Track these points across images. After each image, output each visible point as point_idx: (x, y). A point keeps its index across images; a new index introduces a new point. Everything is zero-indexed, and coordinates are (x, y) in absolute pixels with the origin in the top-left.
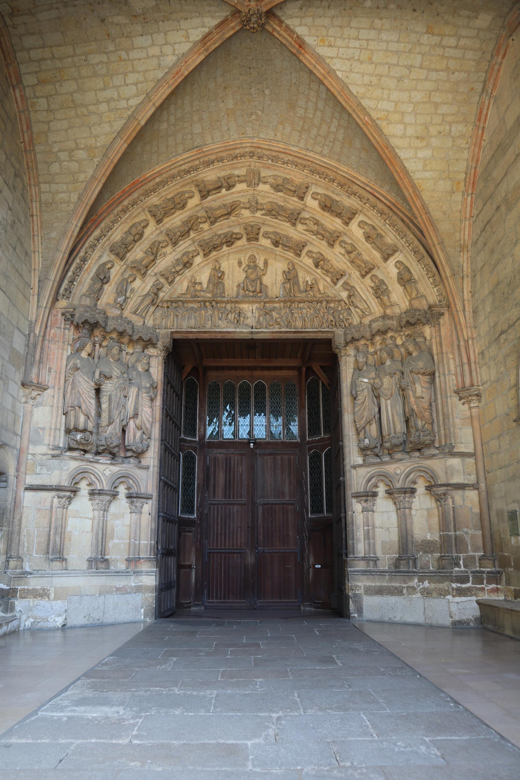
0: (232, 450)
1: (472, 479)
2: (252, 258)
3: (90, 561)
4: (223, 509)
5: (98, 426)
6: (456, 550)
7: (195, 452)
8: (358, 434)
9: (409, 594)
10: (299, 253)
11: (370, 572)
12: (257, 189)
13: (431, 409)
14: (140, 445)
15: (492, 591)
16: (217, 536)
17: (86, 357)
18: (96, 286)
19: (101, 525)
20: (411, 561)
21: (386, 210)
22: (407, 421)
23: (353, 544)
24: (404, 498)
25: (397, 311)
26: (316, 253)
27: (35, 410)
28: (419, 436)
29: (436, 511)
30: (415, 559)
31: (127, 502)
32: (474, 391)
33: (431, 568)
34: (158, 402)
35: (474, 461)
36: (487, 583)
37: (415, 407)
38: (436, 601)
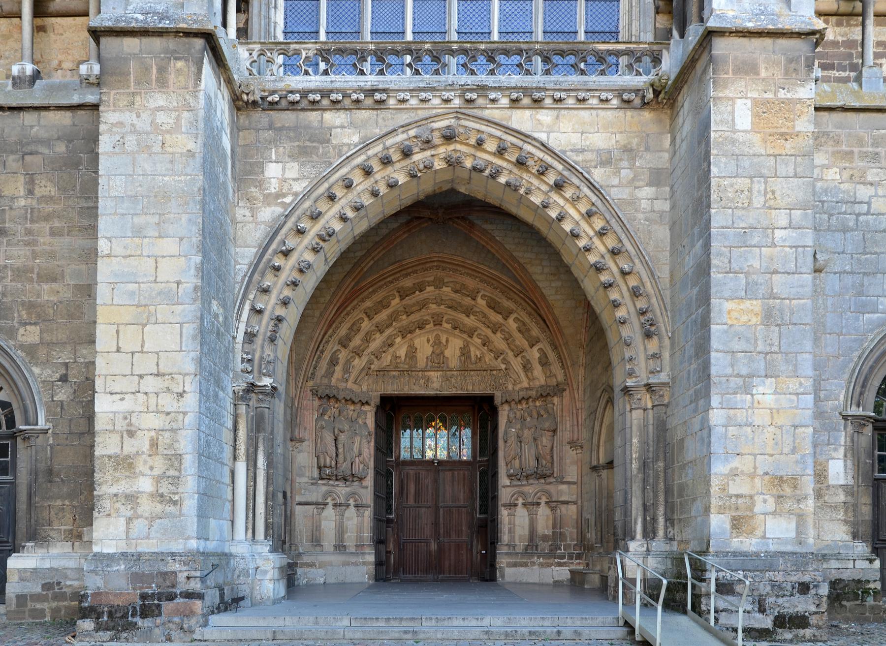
3: (335, 546)
21: (533, 312)
25: (537, 383)
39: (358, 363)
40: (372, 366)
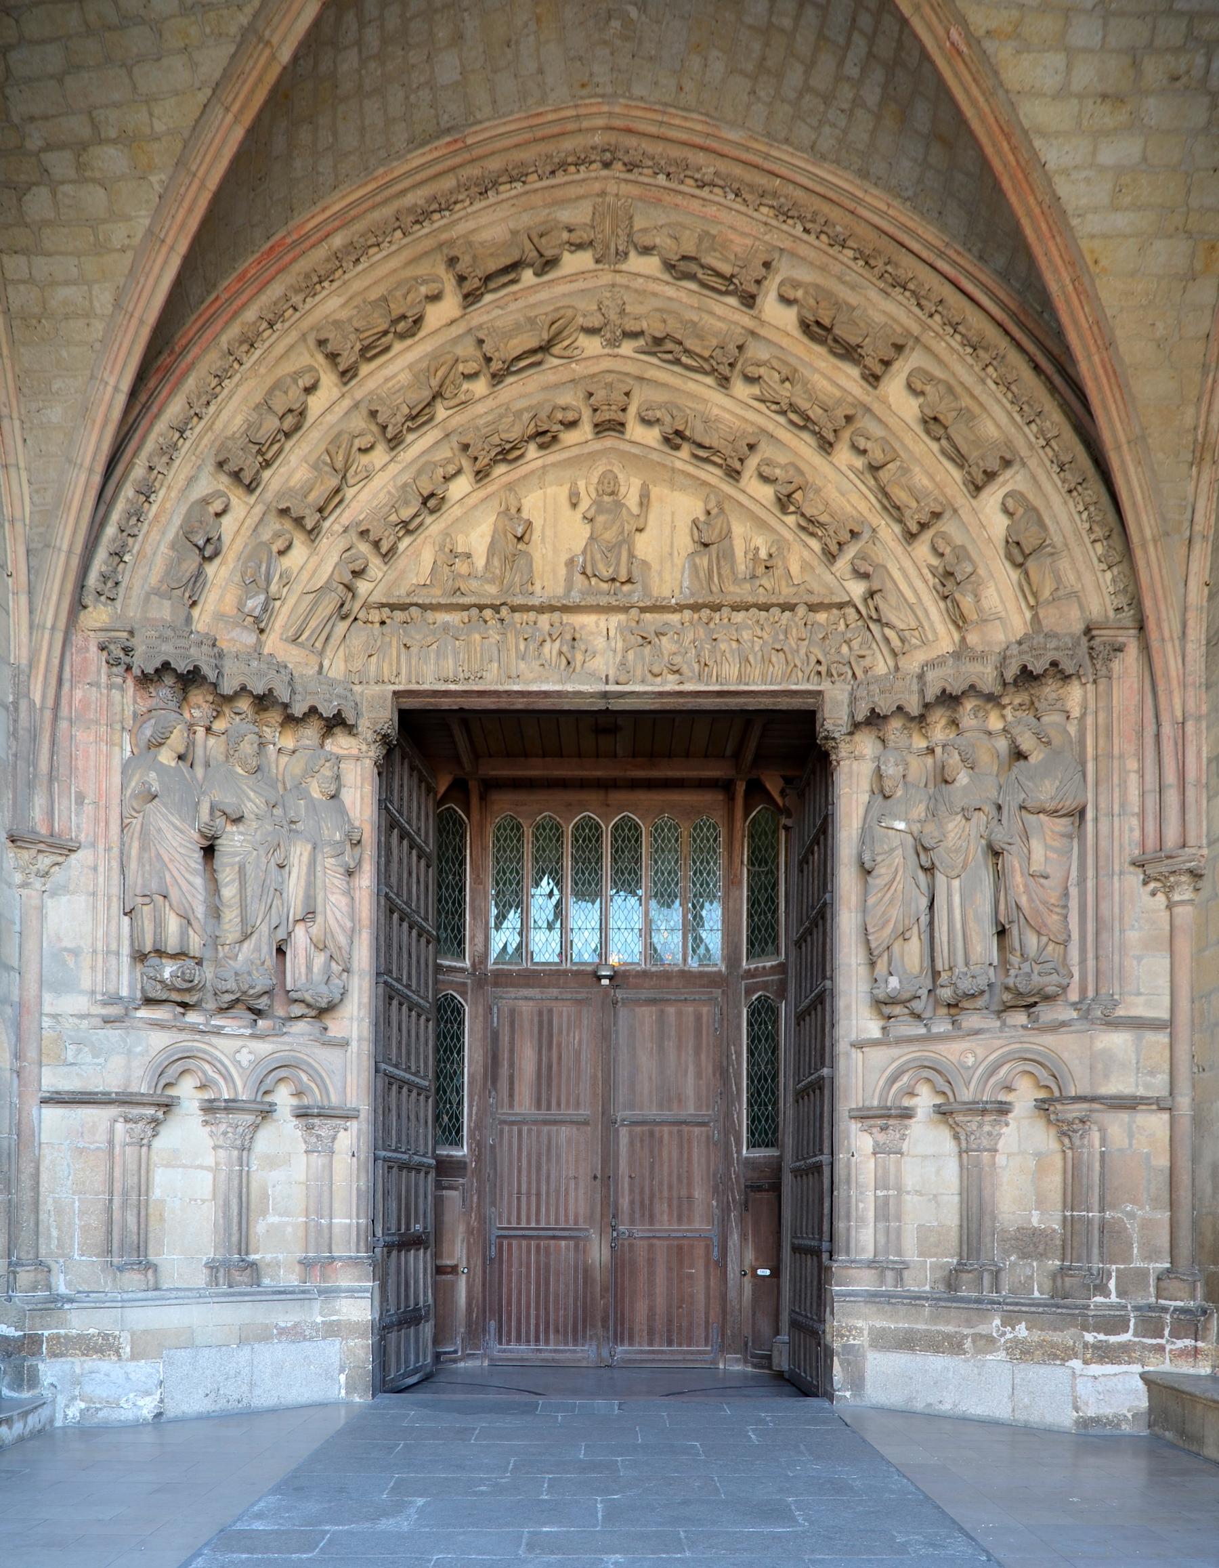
0: (554, 992)
1: (1158, 1085)
2: (609, 488)
3: (212, 1267)
4: (534, 1134)
5: (215, 941)
6: (1101, 1254)
7: (463, 994)
8: (872, 964)
9: (979, 1351)
10: (737, 465)
11: (888, 1296)
12: (624, 267)
13: (1065, 907)
14: (323, 989)
15: (1183, 1353)
16: (519, 1199)
17: (173, 764)
18: (185, 566)
19: (236, 1182)
20: (986, 1276)
22: (1002, 933)
23: (848, 1229)
24: (980, 1126)
26: (784, 467)
27: (50, 903)
28: (1029, 975)
29: (1058, 1160)
30: (998, 1272)
31: (296, 1127)
32: (1186, 860)
33: (1036, 1294)
34: (366, 880)
35: (1167, 1040)
36: (1171, 1335)
37: (1023, 901)
38: (1044, 1370)
39: (311, 564)
40: (363, 587)
